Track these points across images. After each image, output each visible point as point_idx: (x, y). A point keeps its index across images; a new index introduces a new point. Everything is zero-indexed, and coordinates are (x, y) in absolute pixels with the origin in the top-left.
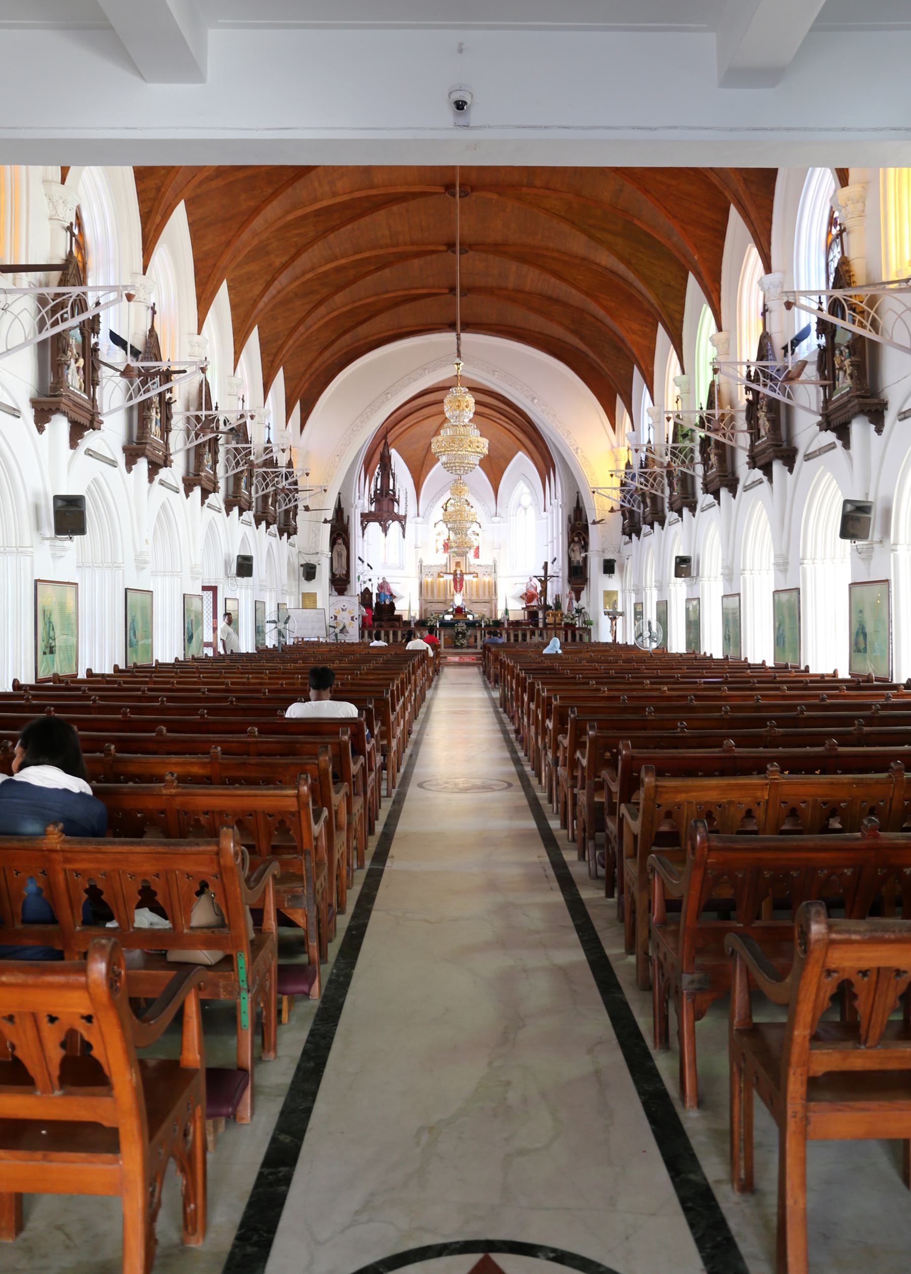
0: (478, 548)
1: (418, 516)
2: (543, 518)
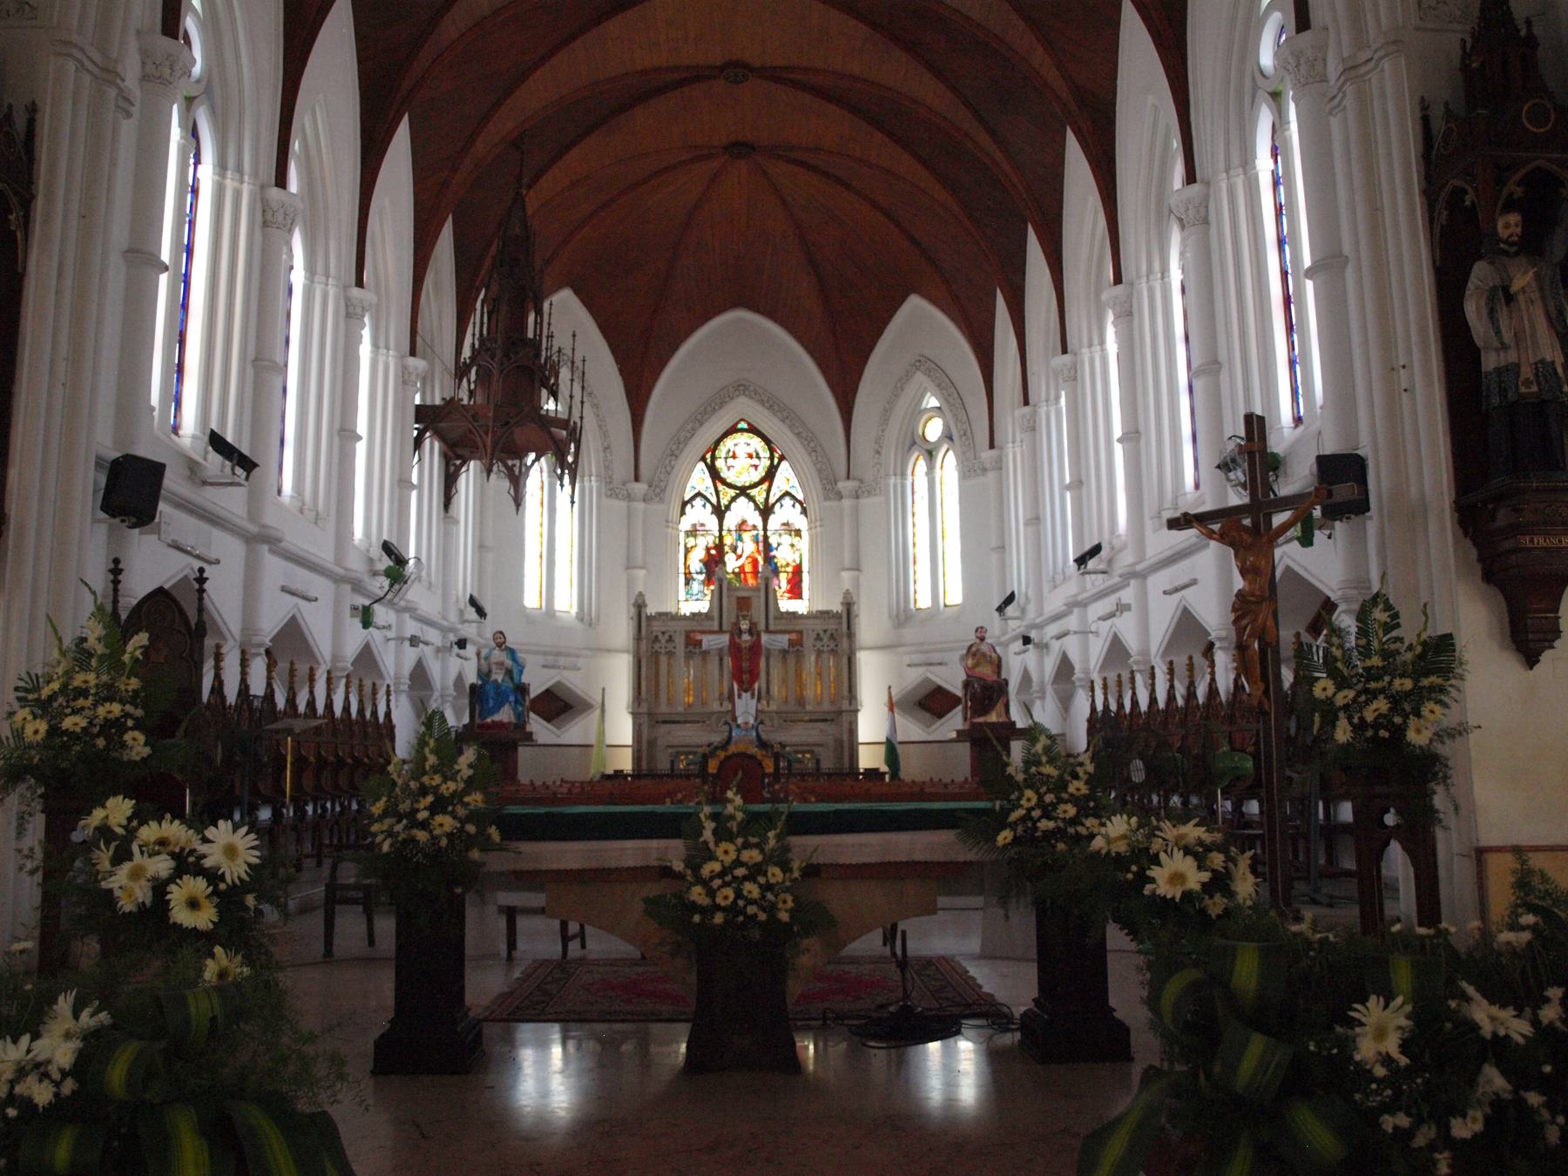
0: (798, 570)
1: (637, 479)
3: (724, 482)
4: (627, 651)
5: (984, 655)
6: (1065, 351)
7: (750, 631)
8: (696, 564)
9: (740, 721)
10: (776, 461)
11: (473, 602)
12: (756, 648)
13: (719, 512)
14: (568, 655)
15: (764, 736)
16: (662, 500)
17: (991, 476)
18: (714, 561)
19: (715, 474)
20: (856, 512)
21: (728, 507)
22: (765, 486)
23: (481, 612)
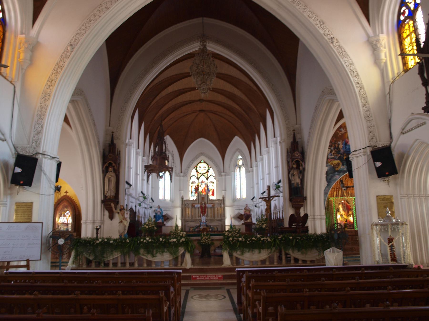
0: (213, 191)
2: (250, 172)
3: (199, 173)
4: (180, 207)
5: (247, 209)
6: (261, 155)
7: (204, 204)
8: (193, 189)
9: (202, 221)
10: (209, 168)
11: (152, 199)
12: (205, 207)
13: (198, 179)
14: (168, 208)
15: (207, 224)
16: (186, 177)
17: (251, 173)
18: (197, 189)
19: (197, 171)
20: (225, 179)
21: (199, 178)
22: (207, 173)
23: (153, 201)
